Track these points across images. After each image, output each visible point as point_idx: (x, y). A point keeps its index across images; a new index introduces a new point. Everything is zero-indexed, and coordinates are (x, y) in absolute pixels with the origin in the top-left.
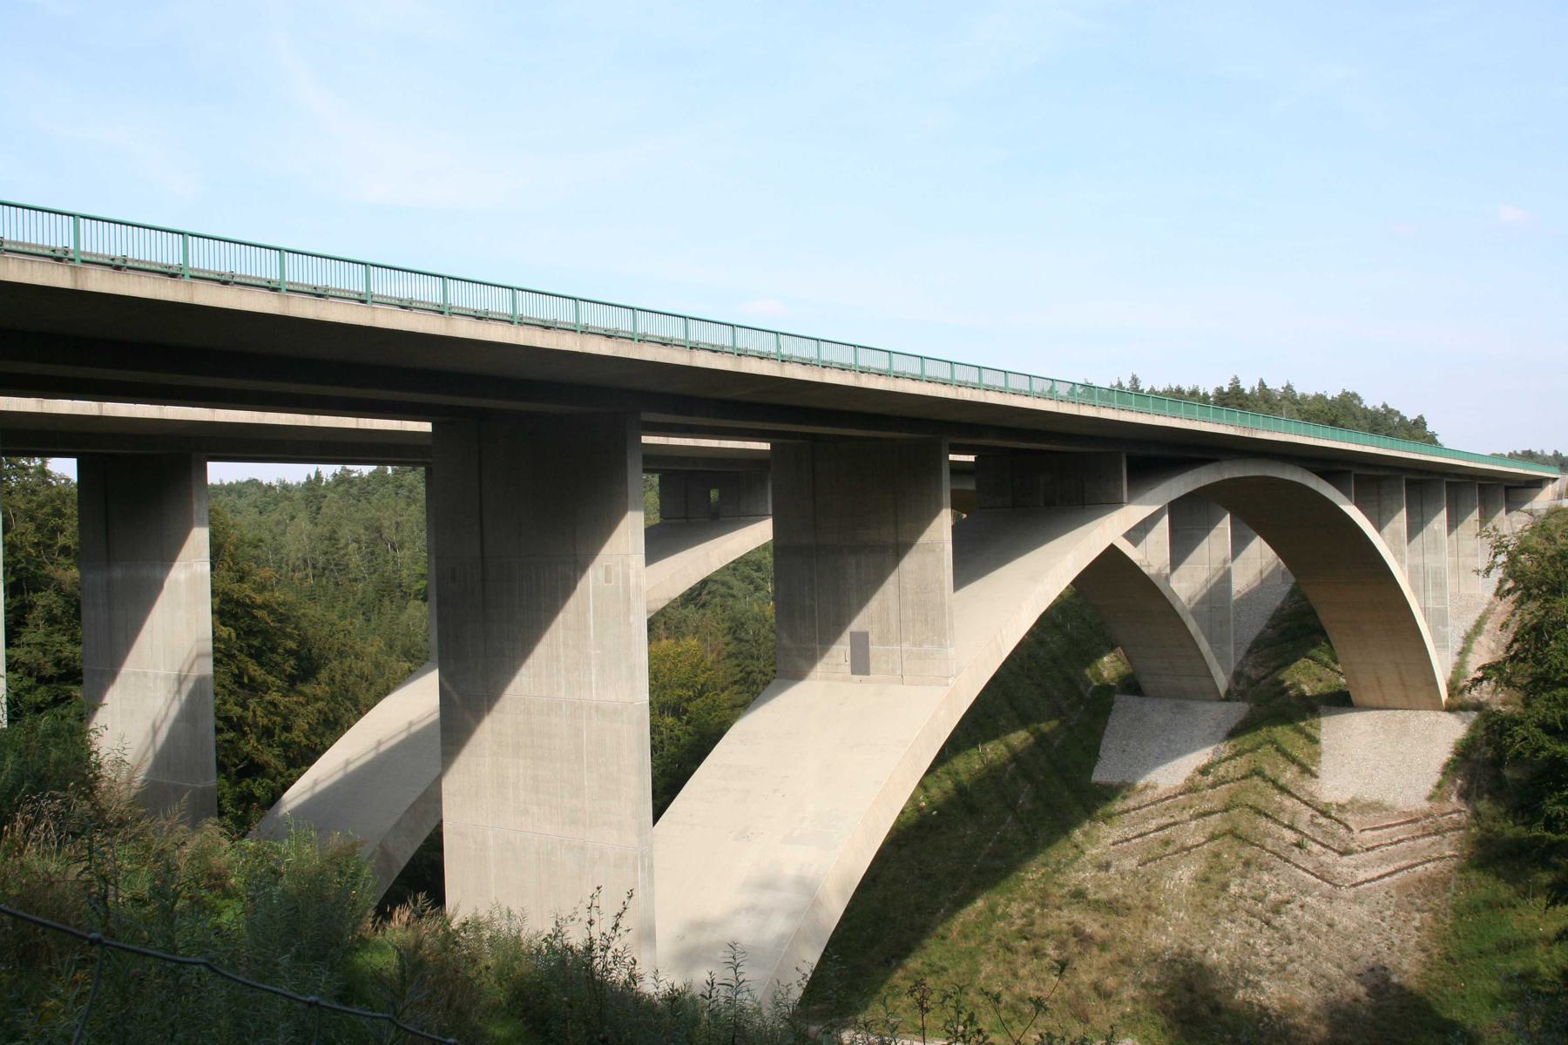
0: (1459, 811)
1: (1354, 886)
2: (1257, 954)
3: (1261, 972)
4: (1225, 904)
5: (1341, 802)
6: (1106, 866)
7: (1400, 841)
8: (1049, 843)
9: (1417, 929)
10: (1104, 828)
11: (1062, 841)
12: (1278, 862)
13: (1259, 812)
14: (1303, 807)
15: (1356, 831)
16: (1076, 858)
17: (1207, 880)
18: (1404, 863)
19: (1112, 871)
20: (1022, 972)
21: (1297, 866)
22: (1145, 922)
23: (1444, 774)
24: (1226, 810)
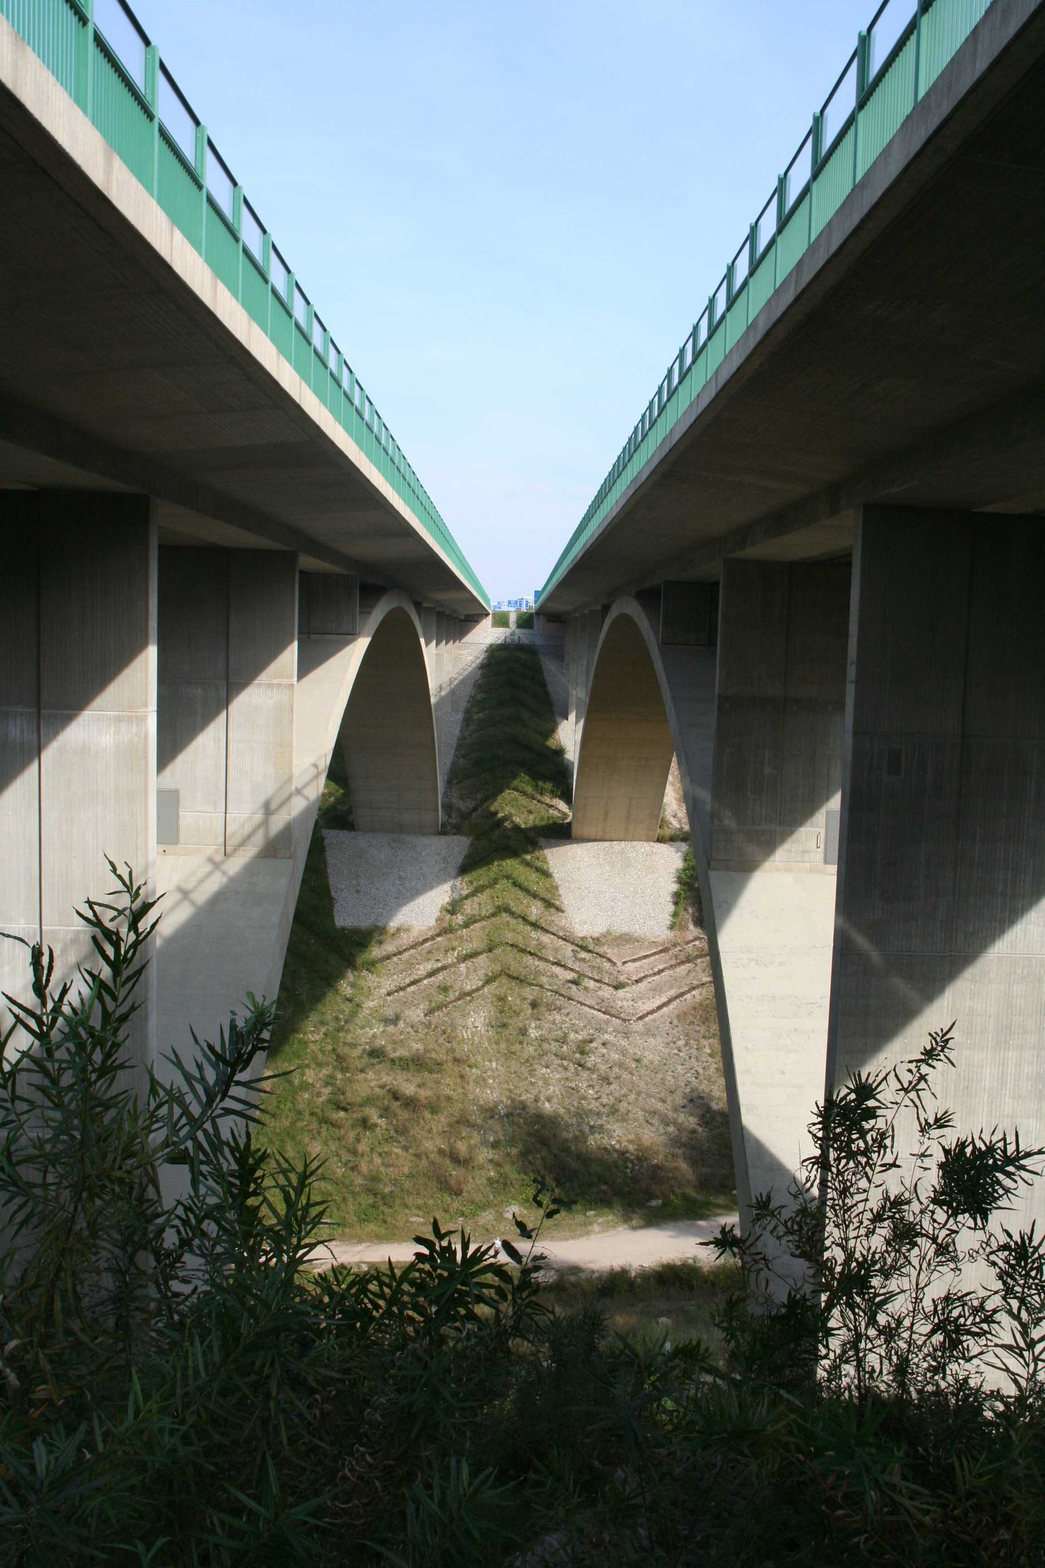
0: (700, 939)
1: (641, 1018)
2: (584, 1098)
3: (599, 1114)
4: (531, 1049)
5: (596, 935)
6: (395, 1020)
7: (660, 971)
8: (317, 998)
9: (710, 1055)
10: (370, 979)
11: (330, 995)
12: (560, 1001)
13: (523, 951)
14: (561, 942)
15: (619, 964)
16: (354, 1014)
17: (504, 1026)
18: (673, 993)
19: (401, 1024)
20: (362, 1147)
21: (582, 1004)
22: (462, 1077)
23: (676, 903)
24: (490, 950)
